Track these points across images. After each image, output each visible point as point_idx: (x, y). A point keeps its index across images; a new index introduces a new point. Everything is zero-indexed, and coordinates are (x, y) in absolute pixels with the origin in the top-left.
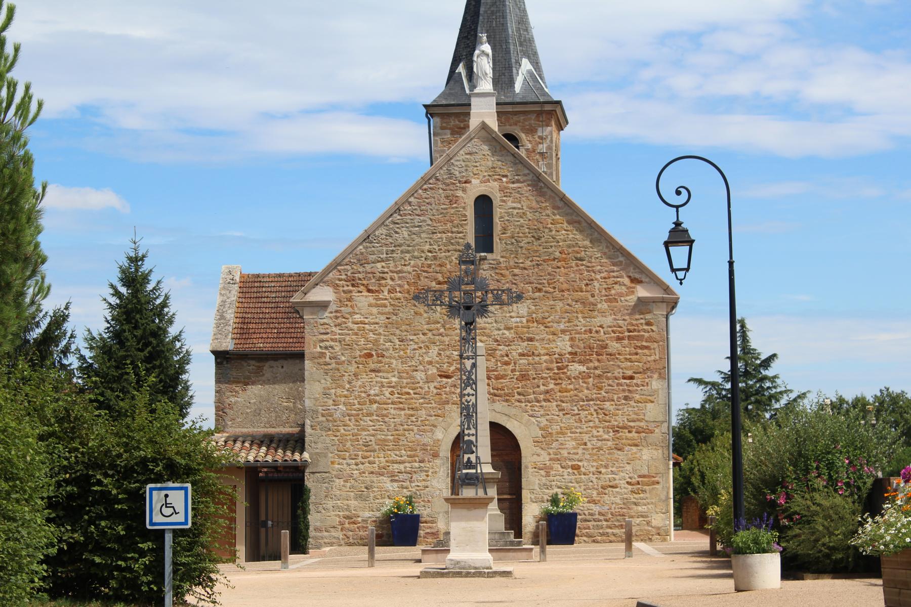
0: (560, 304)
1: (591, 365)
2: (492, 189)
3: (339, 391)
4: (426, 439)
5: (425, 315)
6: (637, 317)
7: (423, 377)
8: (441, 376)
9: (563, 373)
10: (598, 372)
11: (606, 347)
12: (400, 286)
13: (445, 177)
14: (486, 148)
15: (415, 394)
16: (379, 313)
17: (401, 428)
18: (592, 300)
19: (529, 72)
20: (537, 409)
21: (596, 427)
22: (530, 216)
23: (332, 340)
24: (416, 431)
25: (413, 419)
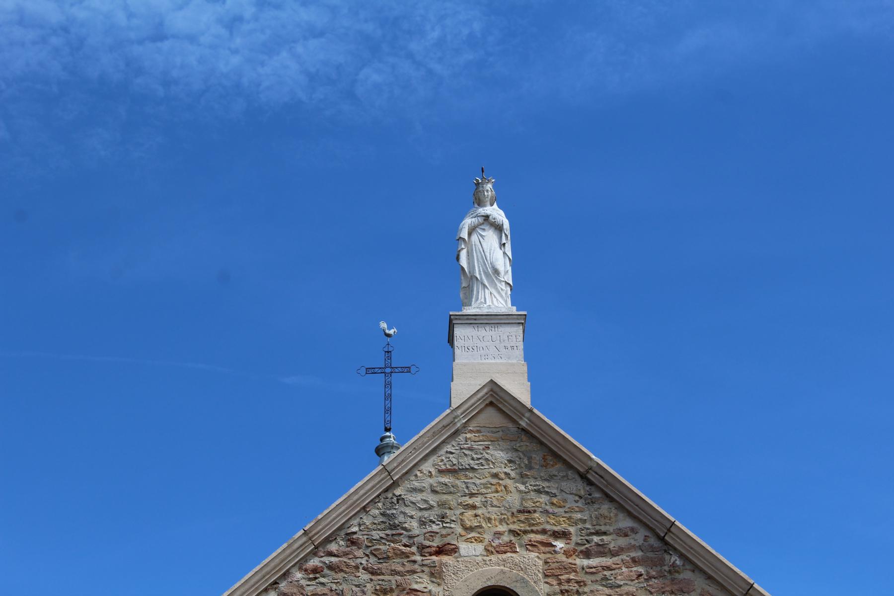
13: (376, 535)
14: (499, 455)
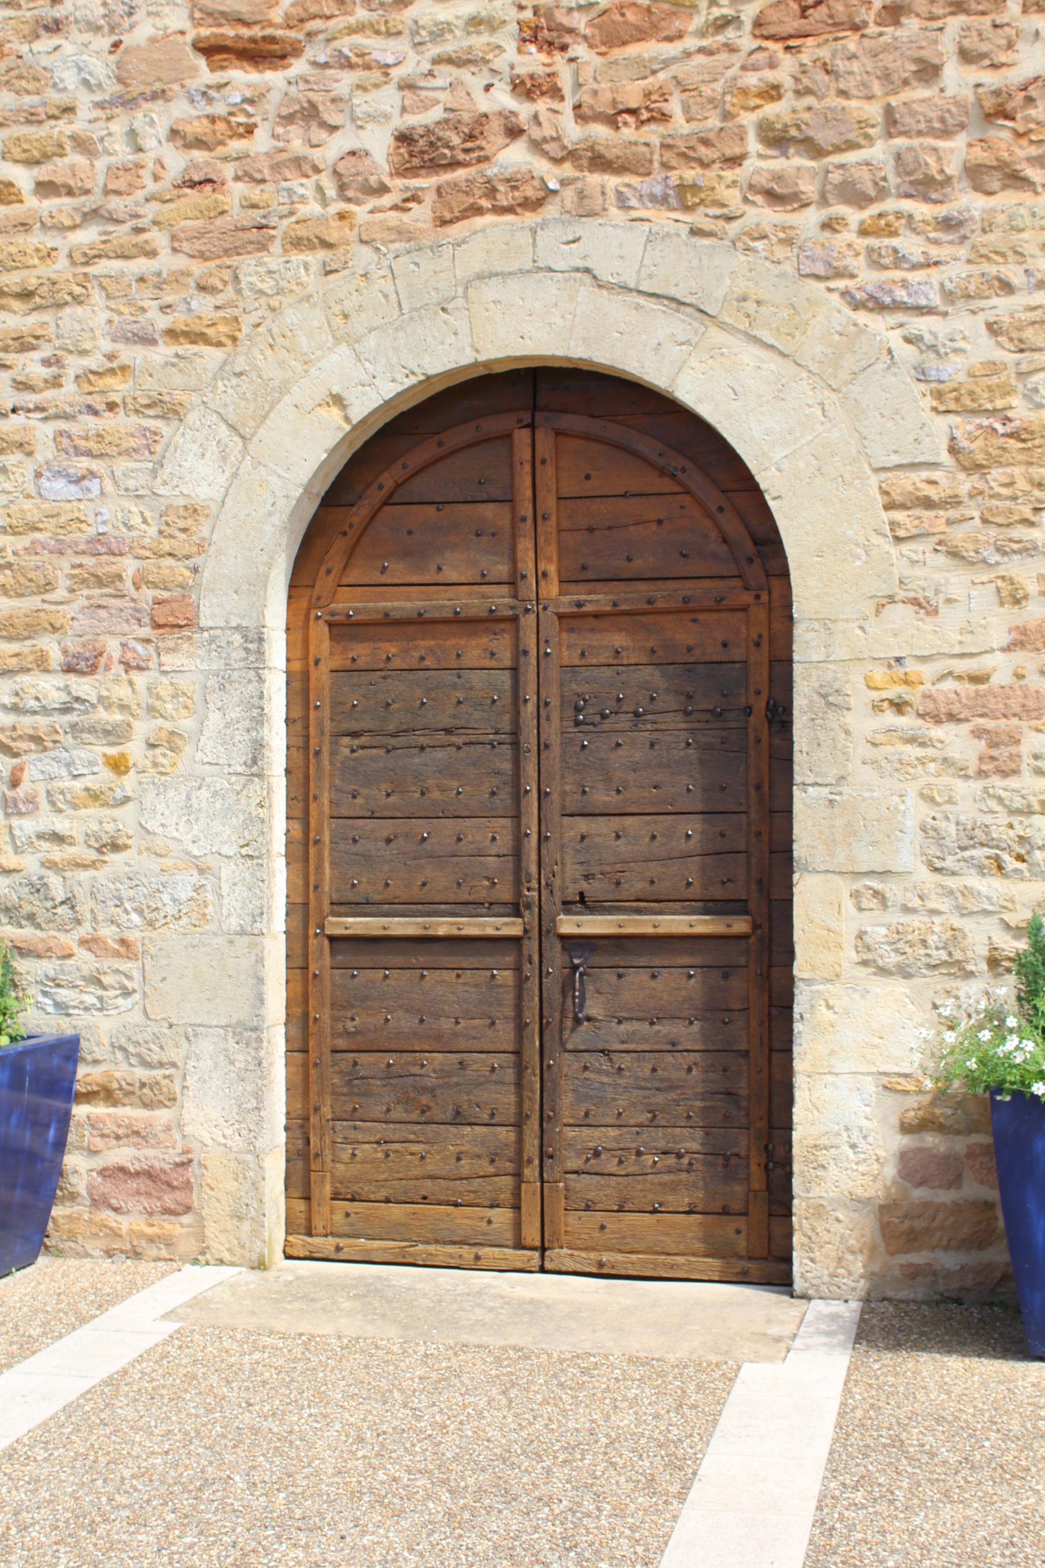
4: (109, 511)
7: (100, 67)
8: (212, 51)
15: (46, 188)
20: (911, 245)
24: (46, 451)
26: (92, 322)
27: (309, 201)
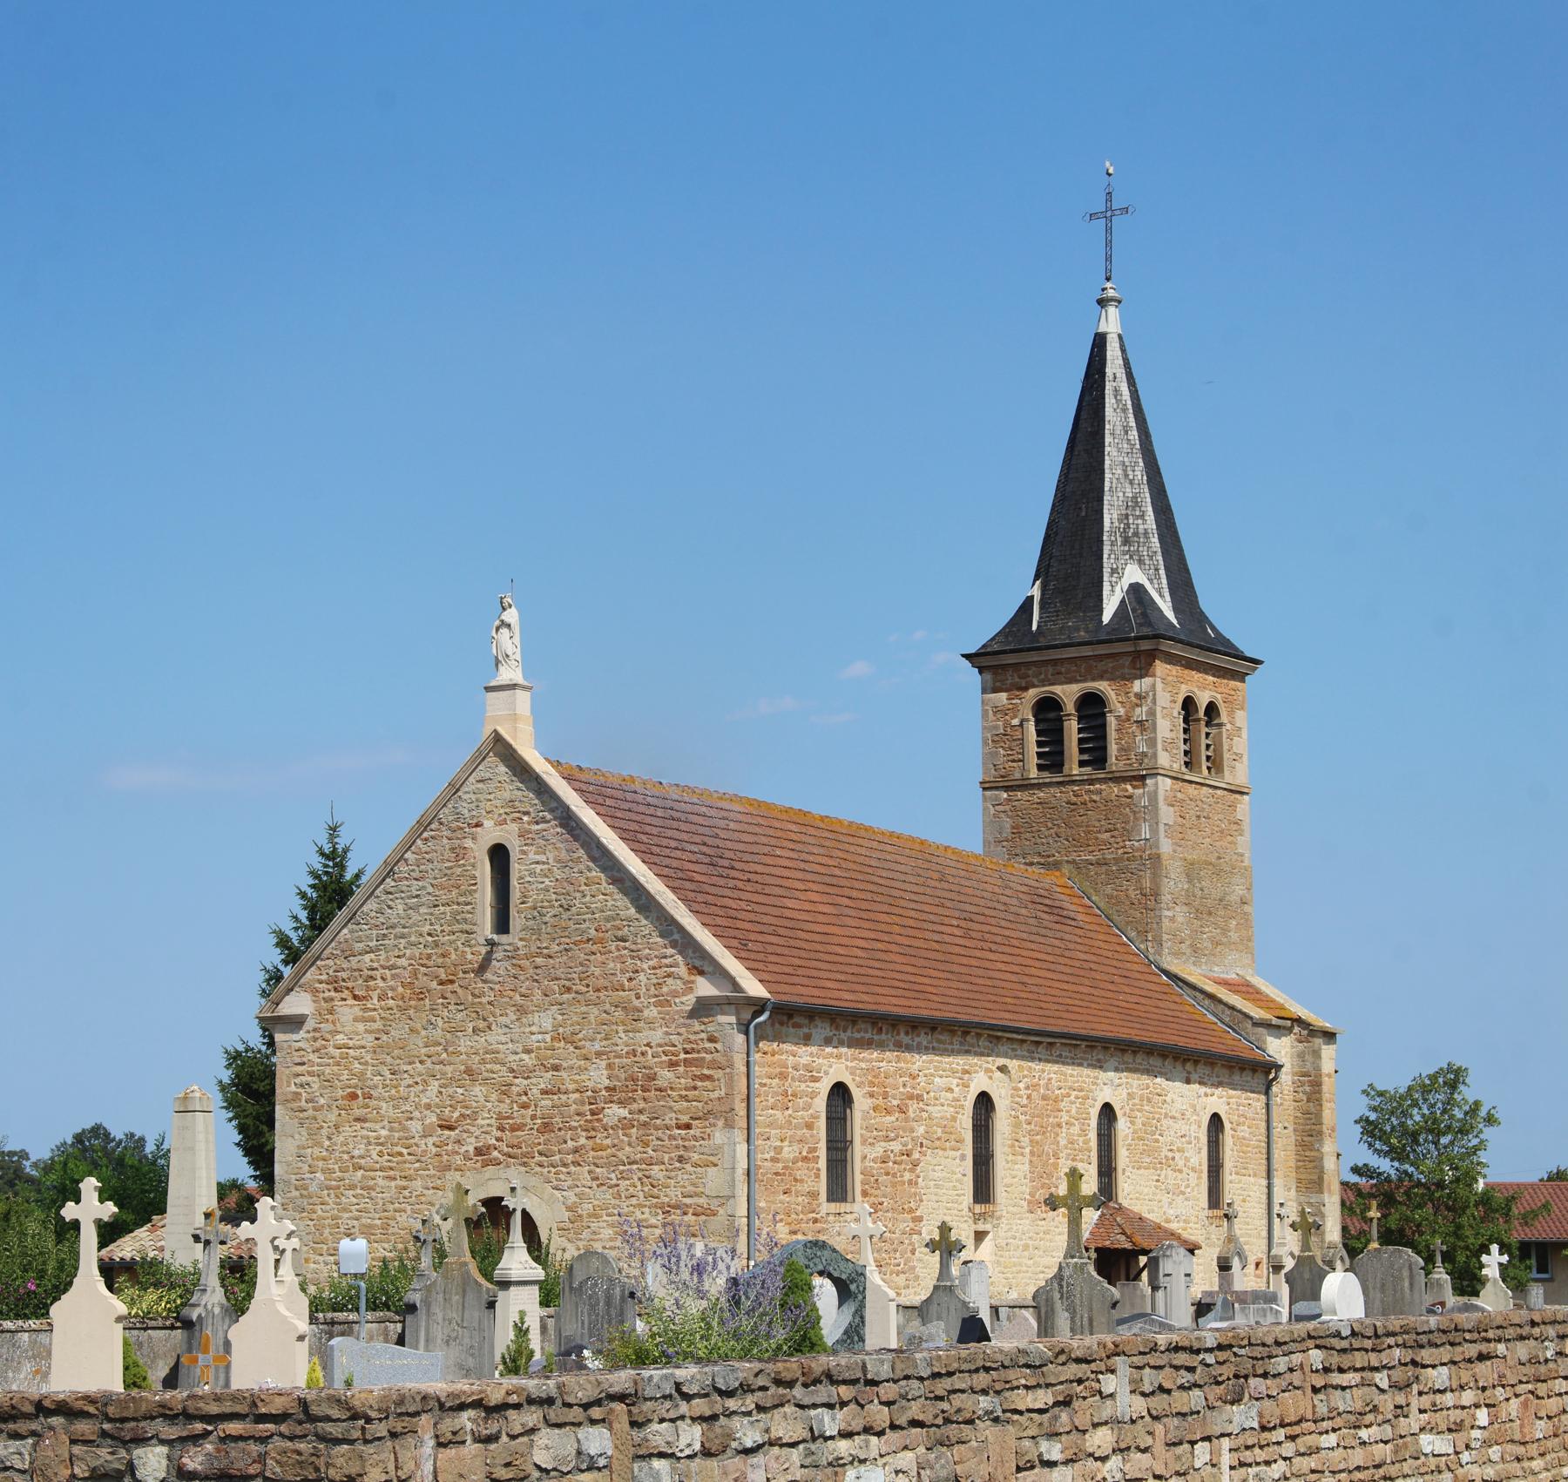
0: (595, 1011)
1: (635, 1106)
2: (508, 835)
3: (316, 1151)
5: (423, 1033)
6: (697, 1027)
7: (420, 1129)
9: (599, 1120)
10: (643, 1118)
11: (653, 1078)
12: (393, 989)
14: (503, 769)
16: (367, 1031)
17: (391, 1207)
18: (636, 1003)
19: (1136, 590)
21: (641, 1206)
22: (558, 874)
23: (309, 1073)
25: (406, 1193)
26: (418, 1184)
27: (458, 1160)
